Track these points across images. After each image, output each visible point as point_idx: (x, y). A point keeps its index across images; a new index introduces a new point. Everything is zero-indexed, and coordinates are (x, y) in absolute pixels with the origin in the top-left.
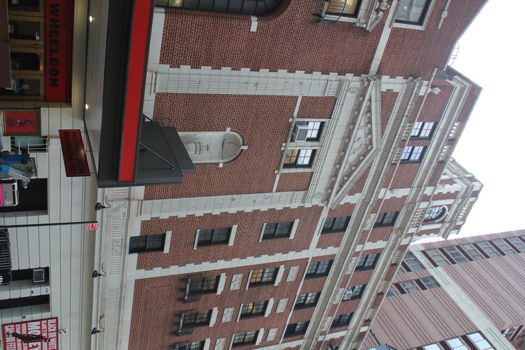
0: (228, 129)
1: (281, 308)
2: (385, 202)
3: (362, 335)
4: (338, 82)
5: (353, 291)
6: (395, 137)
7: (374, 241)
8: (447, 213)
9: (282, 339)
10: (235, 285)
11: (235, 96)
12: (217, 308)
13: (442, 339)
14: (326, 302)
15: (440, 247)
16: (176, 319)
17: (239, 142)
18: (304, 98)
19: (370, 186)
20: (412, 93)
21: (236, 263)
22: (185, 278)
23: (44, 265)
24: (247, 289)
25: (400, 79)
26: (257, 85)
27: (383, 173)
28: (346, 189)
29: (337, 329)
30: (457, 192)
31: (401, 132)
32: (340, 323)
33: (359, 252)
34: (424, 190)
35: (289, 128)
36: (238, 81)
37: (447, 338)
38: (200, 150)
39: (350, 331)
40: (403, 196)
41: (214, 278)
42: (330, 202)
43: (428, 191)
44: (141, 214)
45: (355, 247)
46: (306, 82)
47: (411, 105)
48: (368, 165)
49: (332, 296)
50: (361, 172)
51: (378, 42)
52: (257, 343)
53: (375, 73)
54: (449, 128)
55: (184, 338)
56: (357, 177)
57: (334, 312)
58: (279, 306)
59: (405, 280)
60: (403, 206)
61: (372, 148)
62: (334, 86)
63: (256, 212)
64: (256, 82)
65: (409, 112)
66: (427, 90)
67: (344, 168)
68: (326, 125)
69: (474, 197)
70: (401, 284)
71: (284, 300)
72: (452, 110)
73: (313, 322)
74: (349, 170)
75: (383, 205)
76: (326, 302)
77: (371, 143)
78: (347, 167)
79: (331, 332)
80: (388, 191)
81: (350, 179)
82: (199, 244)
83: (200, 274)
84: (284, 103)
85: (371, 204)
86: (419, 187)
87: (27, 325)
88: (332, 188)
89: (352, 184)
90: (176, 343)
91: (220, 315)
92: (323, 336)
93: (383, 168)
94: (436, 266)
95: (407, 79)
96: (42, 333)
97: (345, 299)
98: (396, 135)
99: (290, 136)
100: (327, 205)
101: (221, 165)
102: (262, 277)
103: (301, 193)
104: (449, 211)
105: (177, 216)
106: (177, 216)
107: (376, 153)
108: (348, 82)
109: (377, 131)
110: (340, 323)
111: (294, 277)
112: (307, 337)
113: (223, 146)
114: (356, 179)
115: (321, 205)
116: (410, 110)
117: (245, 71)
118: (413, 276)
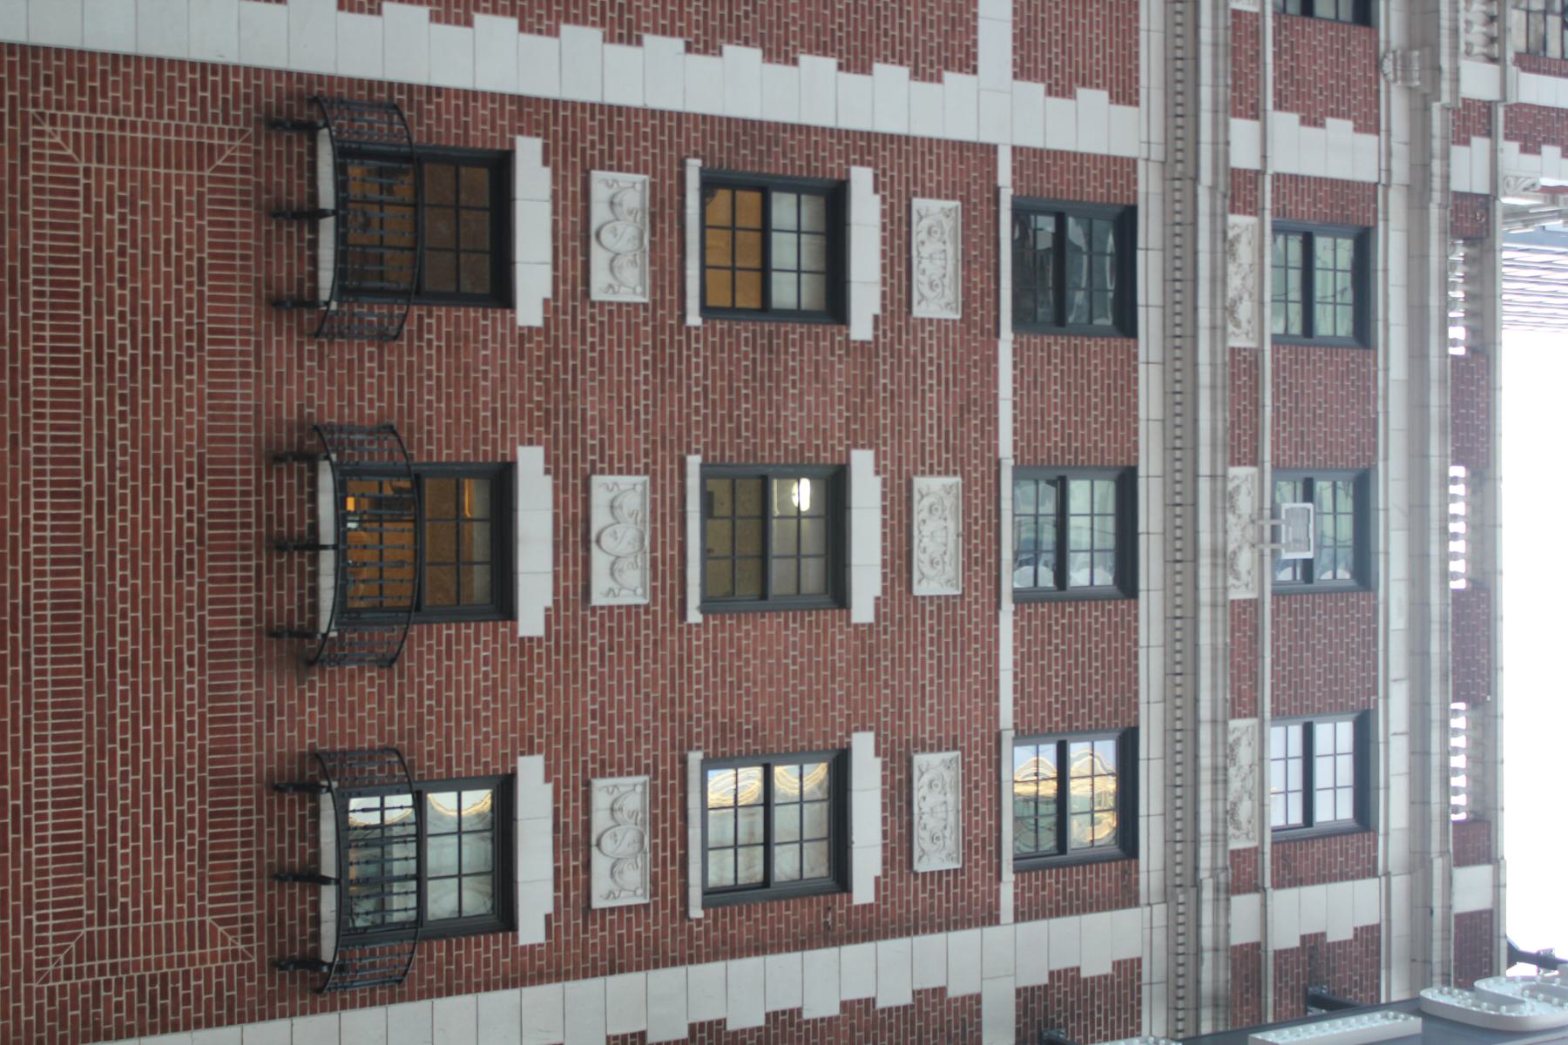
45: (1222, 145)
49: (1204, 486)
60: (1378, 66)
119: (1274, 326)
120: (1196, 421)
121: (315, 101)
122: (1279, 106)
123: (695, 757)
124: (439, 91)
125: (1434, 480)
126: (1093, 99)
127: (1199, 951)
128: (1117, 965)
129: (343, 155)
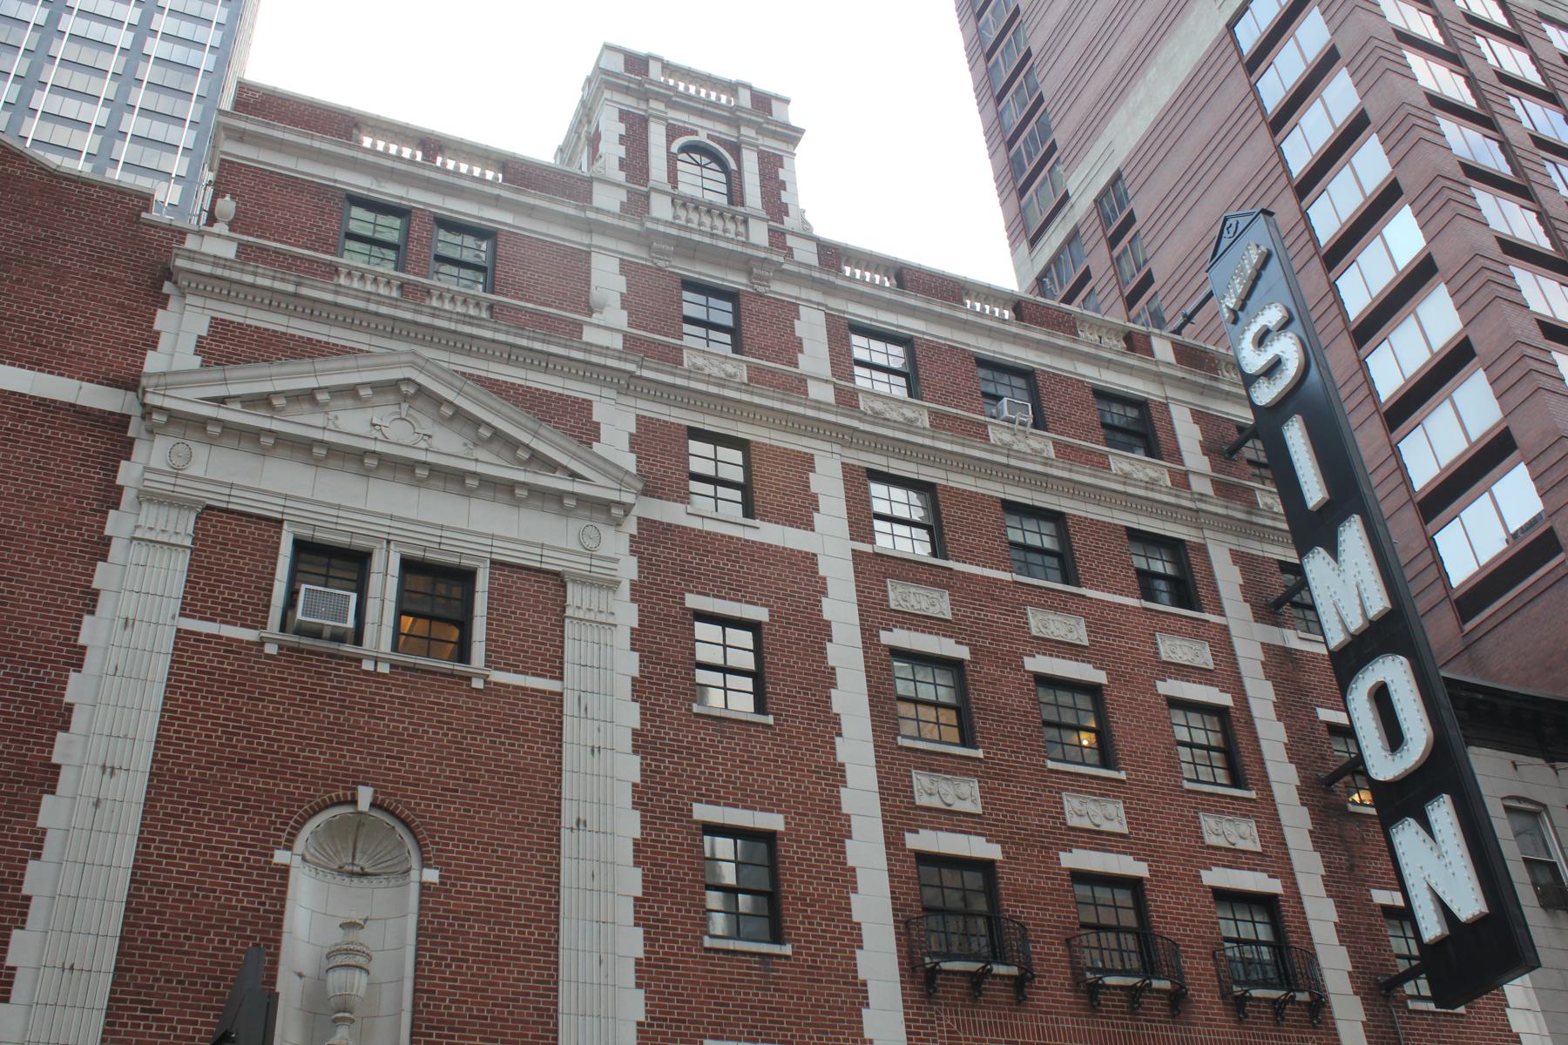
0: (280, 857)
1: (1075, 630)
2: (638, 327)
3: (1188, 356)
4: (145, 505)
5: (998, 398)
6: (377, 314)
7: (798, 346)
8: (702, 137)
9: (1206, 616)
10: (965, 795)
11: (144, 842)
12: (1062, 854)
13: (1264, 131)
14: (1042, 481)
15: (1014, 196)
17: (343, 817)
18: (187, 610)
19: (568, 375)
20: (211, 276)
21: (861, 795)
22: (922, 980)
24: (980, 753)
25: (163, 320)
26: (109, 770)
27: (511, 339)
28: (574, 456)
29: (1161, 435)
30: (624, 116)
31: (356, 297)
32: (1141, 429)
33: (839, 391)
34: (607, 213)
35: (302, 651)
36: (85, 834)
37: (1258, 118)
38: (348, 952)
39: (1172, 393)
40: (623, 271)
41: (930, 872)
42: (614, 496)
43: (608, 199)
45: (819, 405)
46: (128, 607)
47: (255, 274)
48: (470, 387)
50: (498, 406)
51: (13, 393)
52: (1226, 700)
53: (131, 395)
54: (370, 158)
55: (1198, 969)
56: (516, 416)
57: (1090, 452)
58: (1057, 639)
59: (1114, 281)
61: (408, 381)
62: (154, 520)
63: (642, 742)
64: (98, 771)
65: (283, 280)
66: (219, 236)
67: (491, 464)
68: (306, 533)
69: (770, 105)
70: (1127, 292)
71: (1033, 622)
72: (304, 157)
74: (496, 447)
75: (651, 331)
76: (1042, 481)
77: (394, 385)
78: (481, 454)
79: (1176, 455)
80: (596, 318)
81: (525, 438)
82: (777, 938)
83: (904, 927)
84: (195, 673)
85: (631, 367)
86: (590, 227)
88: (558, 496)
89: (542, 431)
90: (1225, 994)
91: (1235, 858)
92: (1193, 480)
93: (493, 341)
94: (1066, 197)
95: (167, 297)
97: (1029, 419)
98: (366, 312)
99: (334, 646)
100: (627, 508)
101: (432, 876)
102: (936, 705)
103: (575, 596)
104: (694, 133)
105: (639, 1024)
106: (639, 1024)
107: (428, 366)
108: (147, 475)
109: (342, 371)
110: (1141, 429)
111: (935, 593)
112: (1193, 532)
113: (363, 874)
114: (523, 420)
115: (631, 527)
116: (274, 278)
117: (51, 812)
118: (1098, 259)
119: (388, 269)
120: (979, 459)
121: (913, 969)
122: (796, 365)
123: (696, 708)
124: (892, 892)
125: (979, 320)
126: (816, 483)
127: (1227, 517)
128: (1235, 563)
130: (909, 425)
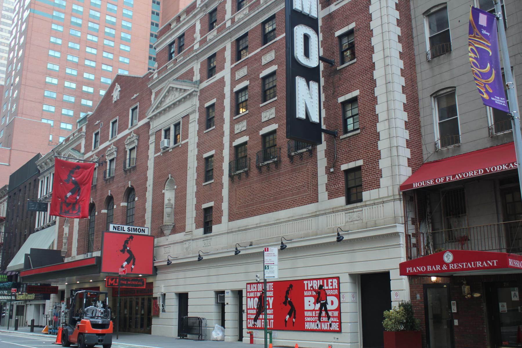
0: (163, 191)
16: (264, 169)
23: (213, 295)
44: (191, 231)
73: (205, 56)
78: (181, 94)
87: (249, 309)
96: (257, 297)
129: (238, 170)
130: (246, 16)
